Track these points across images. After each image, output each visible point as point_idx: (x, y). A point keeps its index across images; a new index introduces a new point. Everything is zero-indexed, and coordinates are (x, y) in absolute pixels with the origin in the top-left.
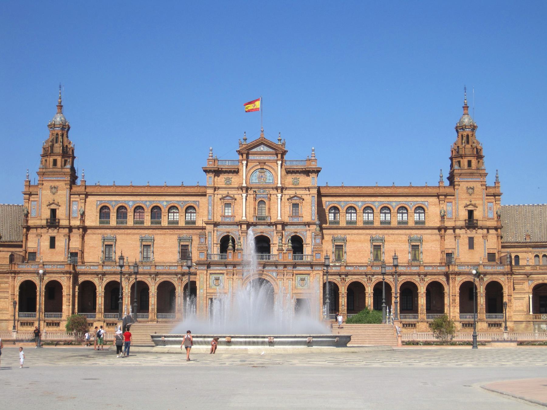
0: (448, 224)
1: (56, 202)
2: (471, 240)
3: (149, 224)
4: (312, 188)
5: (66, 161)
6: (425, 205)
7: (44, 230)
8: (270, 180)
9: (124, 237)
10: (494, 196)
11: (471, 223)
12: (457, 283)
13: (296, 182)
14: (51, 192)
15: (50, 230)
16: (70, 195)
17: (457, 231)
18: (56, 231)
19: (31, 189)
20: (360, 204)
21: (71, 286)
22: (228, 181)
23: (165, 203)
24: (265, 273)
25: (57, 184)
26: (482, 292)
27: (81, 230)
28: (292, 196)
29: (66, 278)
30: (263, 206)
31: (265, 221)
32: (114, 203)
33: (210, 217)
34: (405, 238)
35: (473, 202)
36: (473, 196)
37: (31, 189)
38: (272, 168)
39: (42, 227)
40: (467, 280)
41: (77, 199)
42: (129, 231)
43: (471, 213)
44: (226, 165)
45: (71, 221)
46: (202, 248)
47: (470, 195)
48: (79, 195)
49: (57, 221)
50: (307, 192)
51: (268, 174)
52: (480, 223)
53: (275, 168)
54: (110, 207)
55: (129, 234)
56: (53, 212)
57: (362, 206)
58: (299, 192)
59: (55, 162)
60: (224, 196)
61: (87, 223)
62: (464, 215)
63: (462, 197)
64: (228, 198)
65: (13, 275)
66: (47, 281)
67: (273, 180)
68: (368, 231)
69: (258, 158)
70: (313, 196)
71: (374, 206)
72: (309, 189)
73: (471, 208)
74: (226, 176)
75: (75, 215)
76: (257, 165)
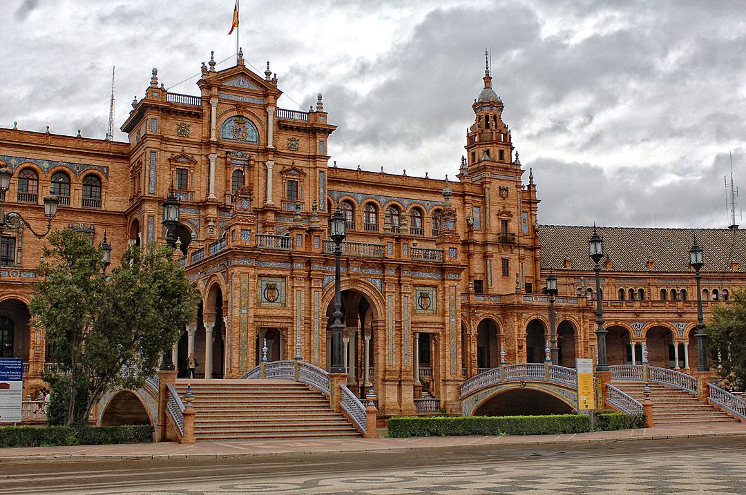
0: (478, 237)
2: (505, 262)
3: (16, 199)
4: (320, 157)
10: (530, 202)
13: (293, 147)
17: (490, 249)
22: (183, 131)
23: (46, 165)
28: (287, 168)
35: (507, 209)
43: (505, 223)
51: (249, 127)
57: (362, 201)
58: (300, 163)
60: (176, 154)
69: (234, 98)
70: (320, 172)
73: (505, 217)
76: (233, 110)
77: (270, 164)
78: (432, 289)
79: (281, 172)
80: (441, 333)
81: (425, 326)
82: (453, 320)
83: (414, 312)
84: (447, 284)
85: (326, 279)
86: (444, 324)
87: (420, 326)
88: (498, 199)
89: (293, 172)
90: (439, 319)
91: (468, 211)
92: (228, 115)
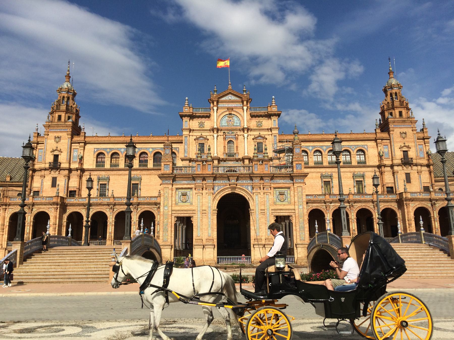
1: (59, 149)
3: (138, 167)
4: (274, 128)
5: (69, 118)
6: (364, 148)
7: (47, 172)
8: (237, 123)
9: (116, 177)
10: (424, 139)
11: (407, 161)
12: (411, 208)
13: (259, 125)
14: (55, 141)
15: (52, 171)
16: (71, 143)
17: (396, 168)
18: (57, 172)
19: (39, 139)
20: (311, 148)
21: (58, 216)
22: (201, 125)
23: (151, 150)
24: (238, 186)
25: (59, 134)
26: (435, 216)
27: (79, 171)
28: (256, 136)
29: (53, 209)
30: (232, 145)
31: (234, 157)
32: (108, 150)
33: (186, 155)
34: (350, 175)
35: (407, 144)
36: (406, 139)
37: (39, 139)
38: (239, 113)
39: (45, 169)
40: (420, 206)
41: (77, 147)
42: (121, 172)
43: (405, 153)
44: (200, 112)
45: (71, 165)
46: (167, 159)
47: (404, 138)
48: (79, 143)
49: (59, 164)
50: (270, 133)
52: (414, 161)
53: (242, 113)
54: (105, 153)
55: (121, 175)
56: (56, 157)
57: (312, 150)
58: (263, 133)
59: (60, 117)
61: (85, 167)
62: (399, 155)
63: (397, 141)
64: (201, 139)
65: (4, 207)
66: (36, 212)
67: (240, 123)
68: (318, 170)
69: (226, 106)
70: (274, 136)
71: (322, 149)
72: (271, 129)
74: (200, 120)
75: (76, 160)
77: (246, 135)
78: (287, 189)
79: (253, 139)
80: (293, 216)
81: (282, 211)
82: (301, 207)
83: (275, 203)
84: (296, 185)
85: (216, 188)
86: (294, 210)
87: (278, 211)
88: (400, 139)
89: (260, 138)
90: (292, 207)
91: (379, 148)
92: (224, 114)
